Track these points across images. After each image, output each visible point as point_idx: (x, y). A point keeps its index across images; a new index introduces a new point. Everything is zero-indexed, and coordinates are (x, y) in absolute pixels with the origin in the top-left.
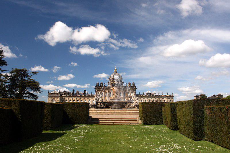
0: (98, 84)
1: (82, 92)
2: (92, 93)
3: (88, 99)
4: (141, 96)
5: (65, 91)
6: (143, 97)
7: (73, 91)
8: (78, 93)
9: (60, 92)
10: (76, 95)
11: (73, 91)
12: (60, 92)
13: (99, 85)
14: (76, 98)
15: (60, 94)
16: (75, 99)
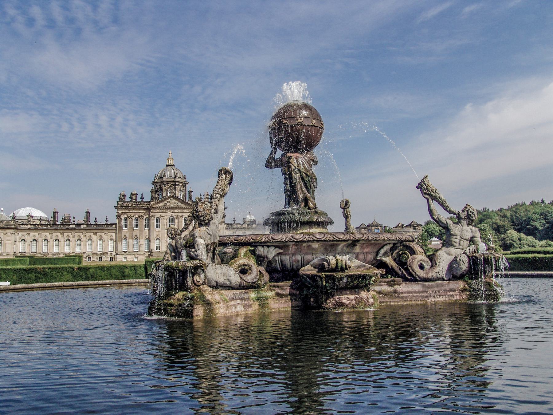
0: (124, 196)
1: (80, 218)
2: (107, 221)
3: (95, 234)
4: (239, 226)
5: (30, 216)
6: (244, 228)
7: (55, 213)
8: (66, 219)
9: (14, 217)
10: (62, 224)
11: (55, 213)
12: (14, 217)
13: (128, 199)
14: (62, 234)
15: (15, 222)
16: (59, 234)
